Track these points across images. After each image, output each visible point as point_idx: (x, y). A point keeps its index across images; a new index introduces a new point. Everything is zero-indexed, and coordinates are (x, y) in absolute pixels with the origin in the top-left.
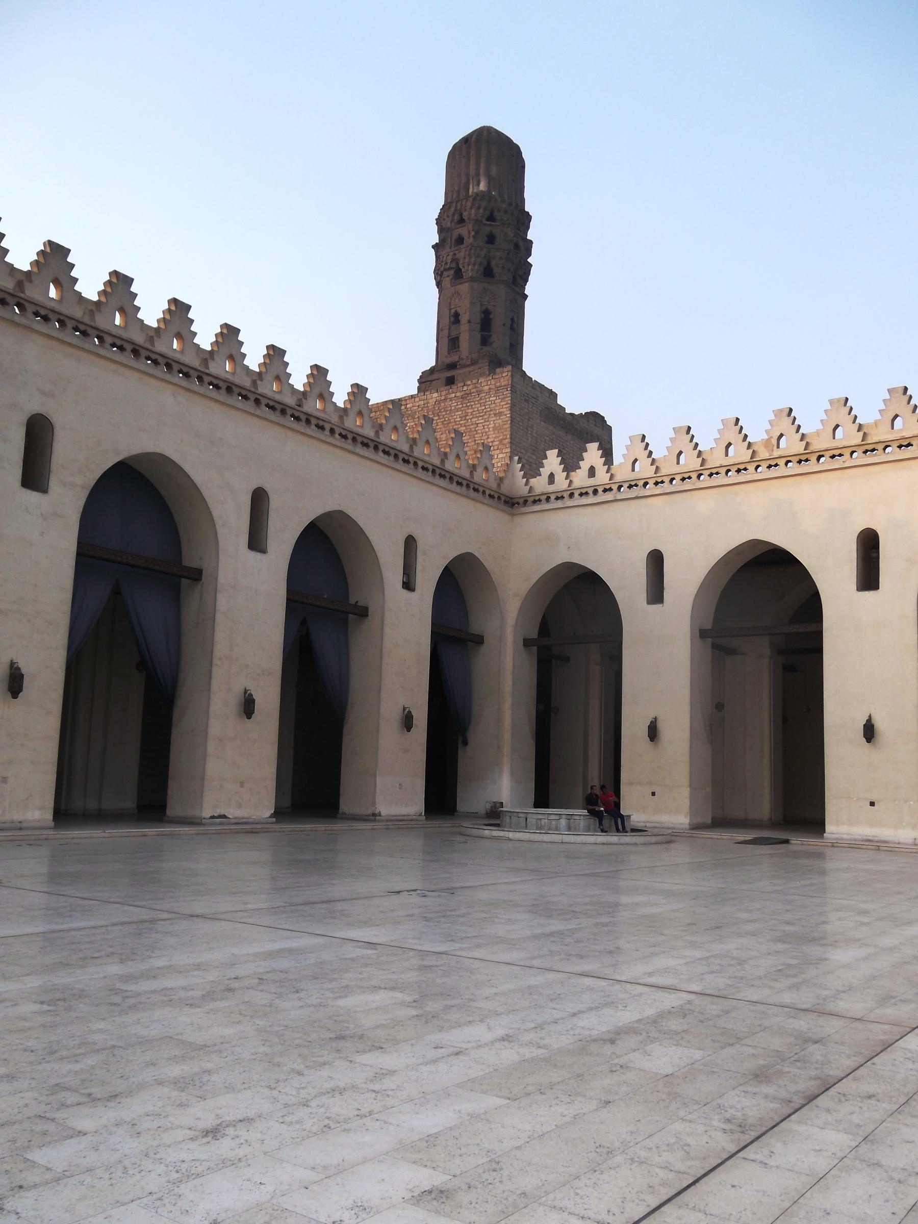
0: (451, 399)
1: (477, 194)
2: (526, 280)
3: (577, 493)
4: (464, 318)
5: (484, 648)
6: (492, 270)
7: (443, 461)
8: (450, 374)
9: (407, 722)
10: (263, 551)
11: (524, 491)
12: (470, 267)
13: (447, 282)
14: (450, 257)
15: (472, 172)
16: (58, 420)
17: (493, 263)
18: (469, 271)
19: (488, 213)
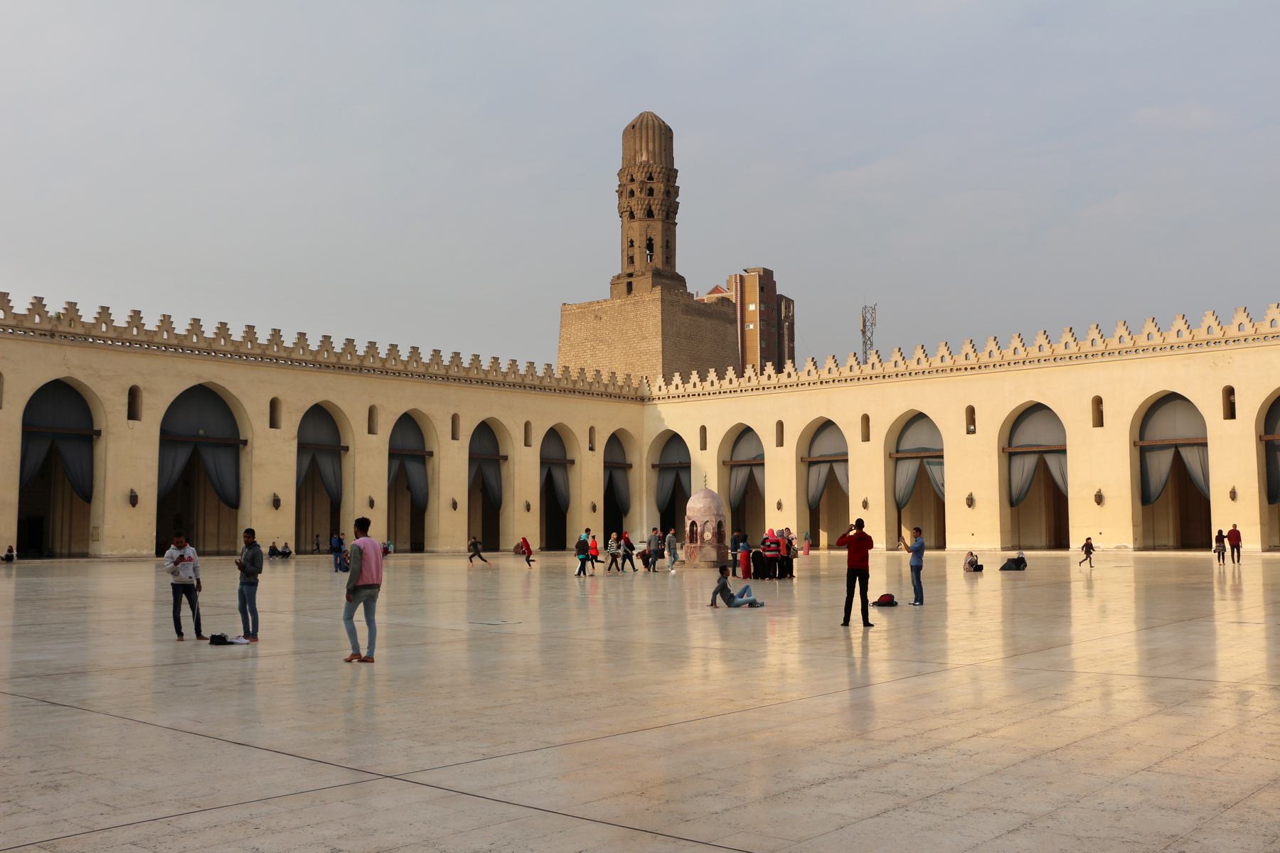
0: (628, 304)
1: (641, 162)
2: (676, 214)
3: (671, 397)
4: (636, 244)
5: (633, 469)
6: (652, 212)
7: (606, 388)
8: (629, 280)
9: (594, 508)
10: (530, 446)
11: (647, 393)
12: (638, 212)
13: (625, 218)
14: (626, 204)
15: (638, 148)
16: (460, 414)
17: (653, 208)
18: (639, 214)
19: (648, 175)
